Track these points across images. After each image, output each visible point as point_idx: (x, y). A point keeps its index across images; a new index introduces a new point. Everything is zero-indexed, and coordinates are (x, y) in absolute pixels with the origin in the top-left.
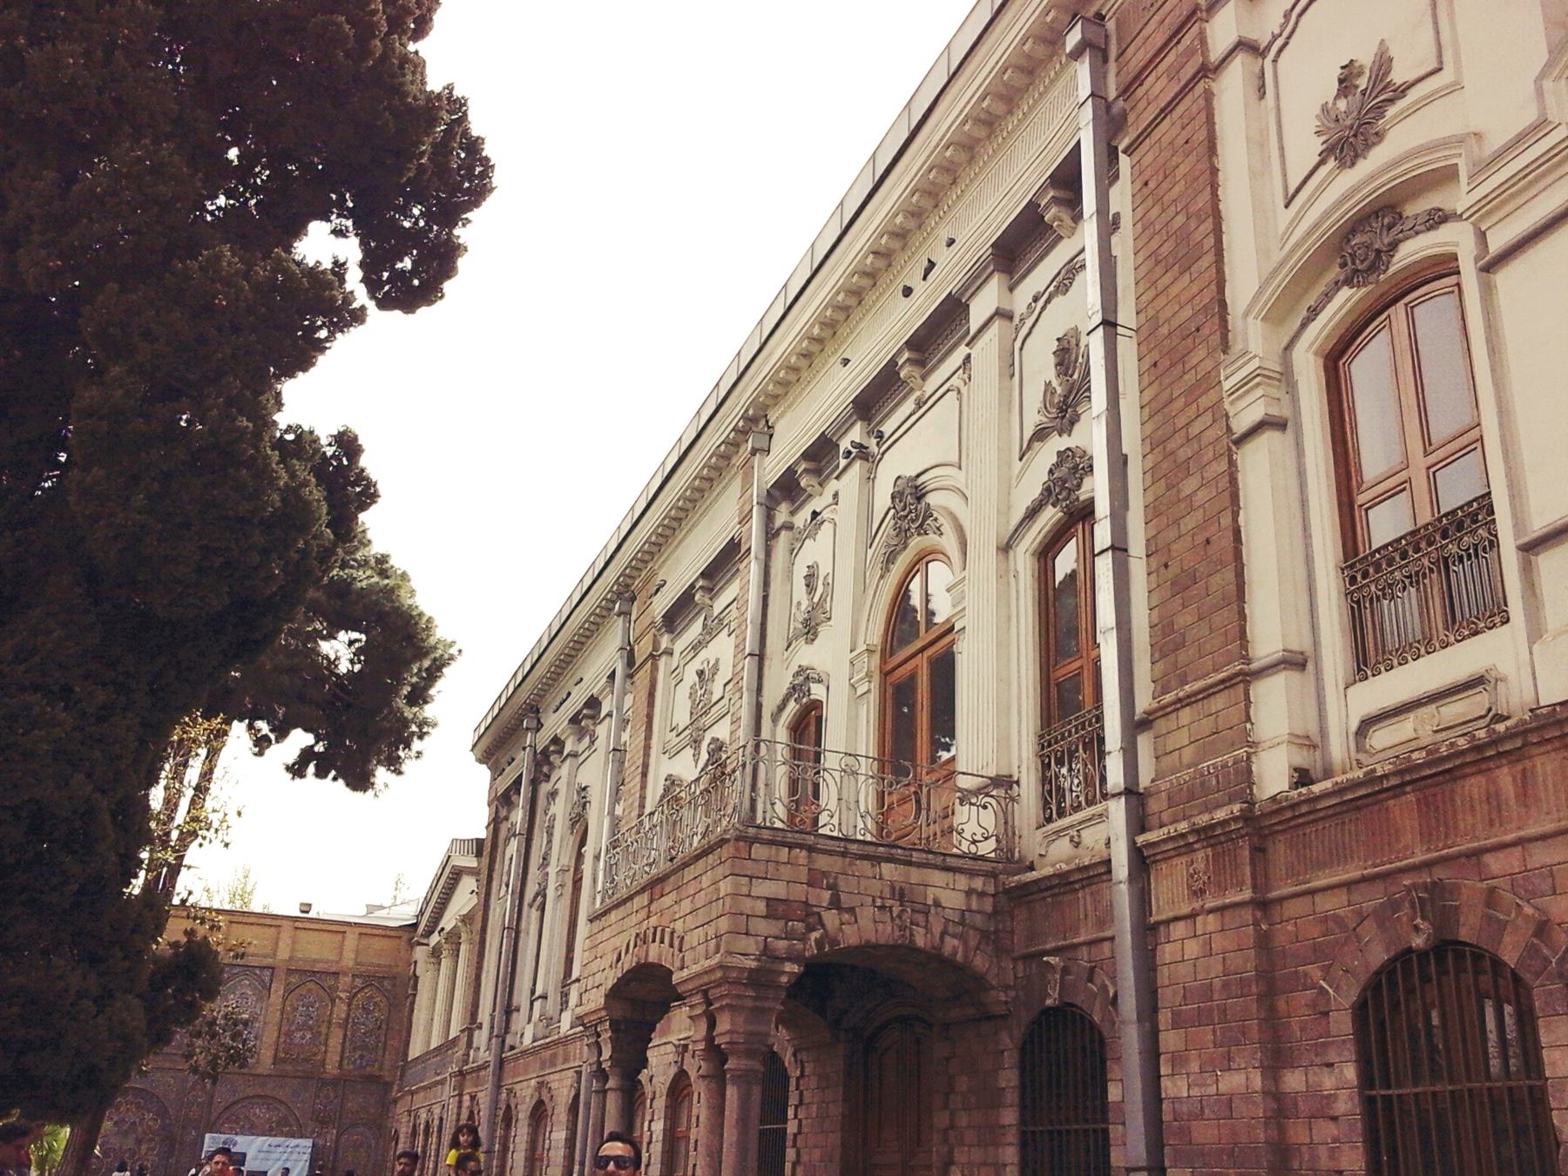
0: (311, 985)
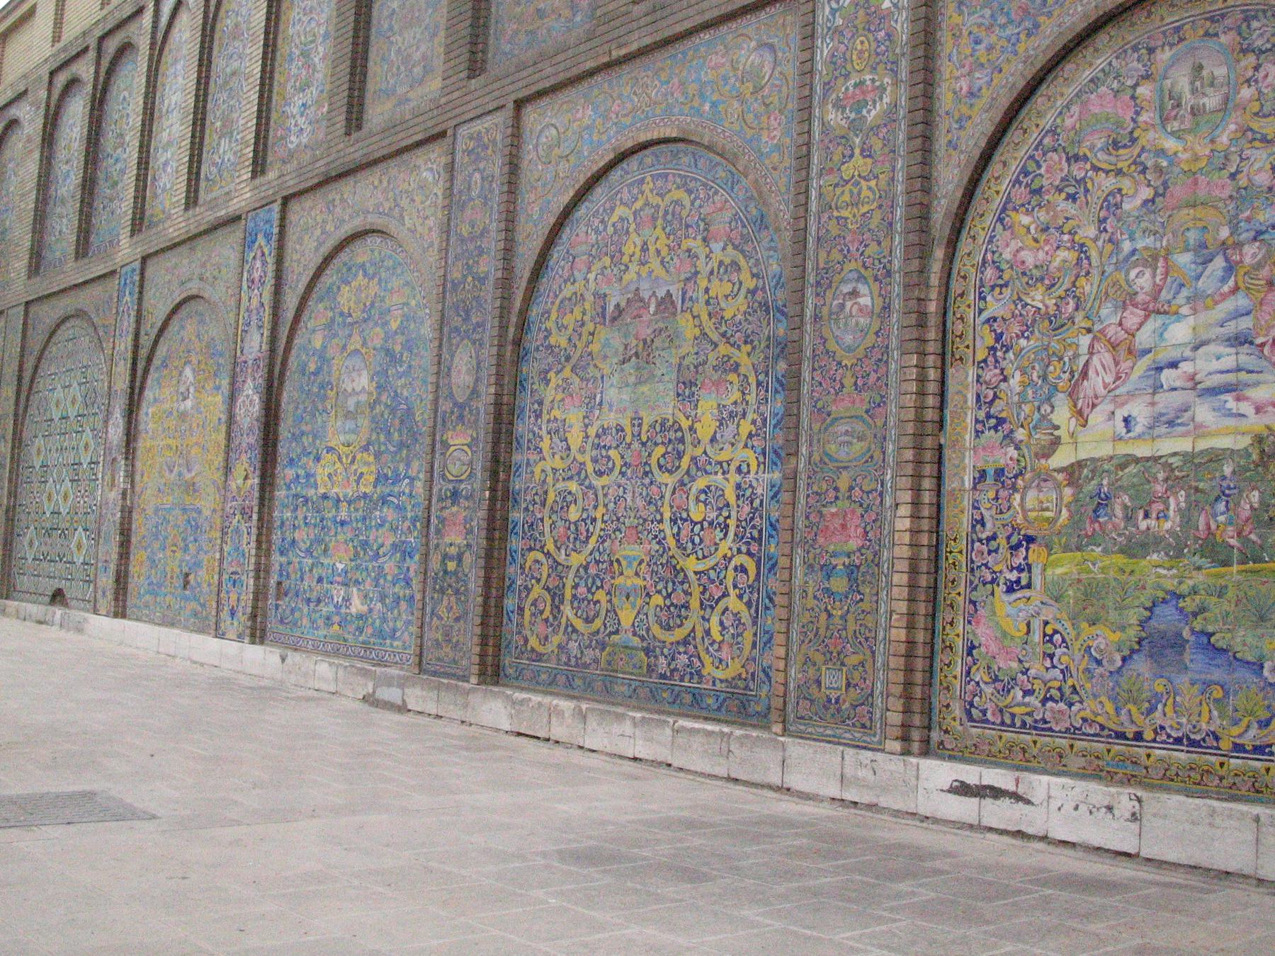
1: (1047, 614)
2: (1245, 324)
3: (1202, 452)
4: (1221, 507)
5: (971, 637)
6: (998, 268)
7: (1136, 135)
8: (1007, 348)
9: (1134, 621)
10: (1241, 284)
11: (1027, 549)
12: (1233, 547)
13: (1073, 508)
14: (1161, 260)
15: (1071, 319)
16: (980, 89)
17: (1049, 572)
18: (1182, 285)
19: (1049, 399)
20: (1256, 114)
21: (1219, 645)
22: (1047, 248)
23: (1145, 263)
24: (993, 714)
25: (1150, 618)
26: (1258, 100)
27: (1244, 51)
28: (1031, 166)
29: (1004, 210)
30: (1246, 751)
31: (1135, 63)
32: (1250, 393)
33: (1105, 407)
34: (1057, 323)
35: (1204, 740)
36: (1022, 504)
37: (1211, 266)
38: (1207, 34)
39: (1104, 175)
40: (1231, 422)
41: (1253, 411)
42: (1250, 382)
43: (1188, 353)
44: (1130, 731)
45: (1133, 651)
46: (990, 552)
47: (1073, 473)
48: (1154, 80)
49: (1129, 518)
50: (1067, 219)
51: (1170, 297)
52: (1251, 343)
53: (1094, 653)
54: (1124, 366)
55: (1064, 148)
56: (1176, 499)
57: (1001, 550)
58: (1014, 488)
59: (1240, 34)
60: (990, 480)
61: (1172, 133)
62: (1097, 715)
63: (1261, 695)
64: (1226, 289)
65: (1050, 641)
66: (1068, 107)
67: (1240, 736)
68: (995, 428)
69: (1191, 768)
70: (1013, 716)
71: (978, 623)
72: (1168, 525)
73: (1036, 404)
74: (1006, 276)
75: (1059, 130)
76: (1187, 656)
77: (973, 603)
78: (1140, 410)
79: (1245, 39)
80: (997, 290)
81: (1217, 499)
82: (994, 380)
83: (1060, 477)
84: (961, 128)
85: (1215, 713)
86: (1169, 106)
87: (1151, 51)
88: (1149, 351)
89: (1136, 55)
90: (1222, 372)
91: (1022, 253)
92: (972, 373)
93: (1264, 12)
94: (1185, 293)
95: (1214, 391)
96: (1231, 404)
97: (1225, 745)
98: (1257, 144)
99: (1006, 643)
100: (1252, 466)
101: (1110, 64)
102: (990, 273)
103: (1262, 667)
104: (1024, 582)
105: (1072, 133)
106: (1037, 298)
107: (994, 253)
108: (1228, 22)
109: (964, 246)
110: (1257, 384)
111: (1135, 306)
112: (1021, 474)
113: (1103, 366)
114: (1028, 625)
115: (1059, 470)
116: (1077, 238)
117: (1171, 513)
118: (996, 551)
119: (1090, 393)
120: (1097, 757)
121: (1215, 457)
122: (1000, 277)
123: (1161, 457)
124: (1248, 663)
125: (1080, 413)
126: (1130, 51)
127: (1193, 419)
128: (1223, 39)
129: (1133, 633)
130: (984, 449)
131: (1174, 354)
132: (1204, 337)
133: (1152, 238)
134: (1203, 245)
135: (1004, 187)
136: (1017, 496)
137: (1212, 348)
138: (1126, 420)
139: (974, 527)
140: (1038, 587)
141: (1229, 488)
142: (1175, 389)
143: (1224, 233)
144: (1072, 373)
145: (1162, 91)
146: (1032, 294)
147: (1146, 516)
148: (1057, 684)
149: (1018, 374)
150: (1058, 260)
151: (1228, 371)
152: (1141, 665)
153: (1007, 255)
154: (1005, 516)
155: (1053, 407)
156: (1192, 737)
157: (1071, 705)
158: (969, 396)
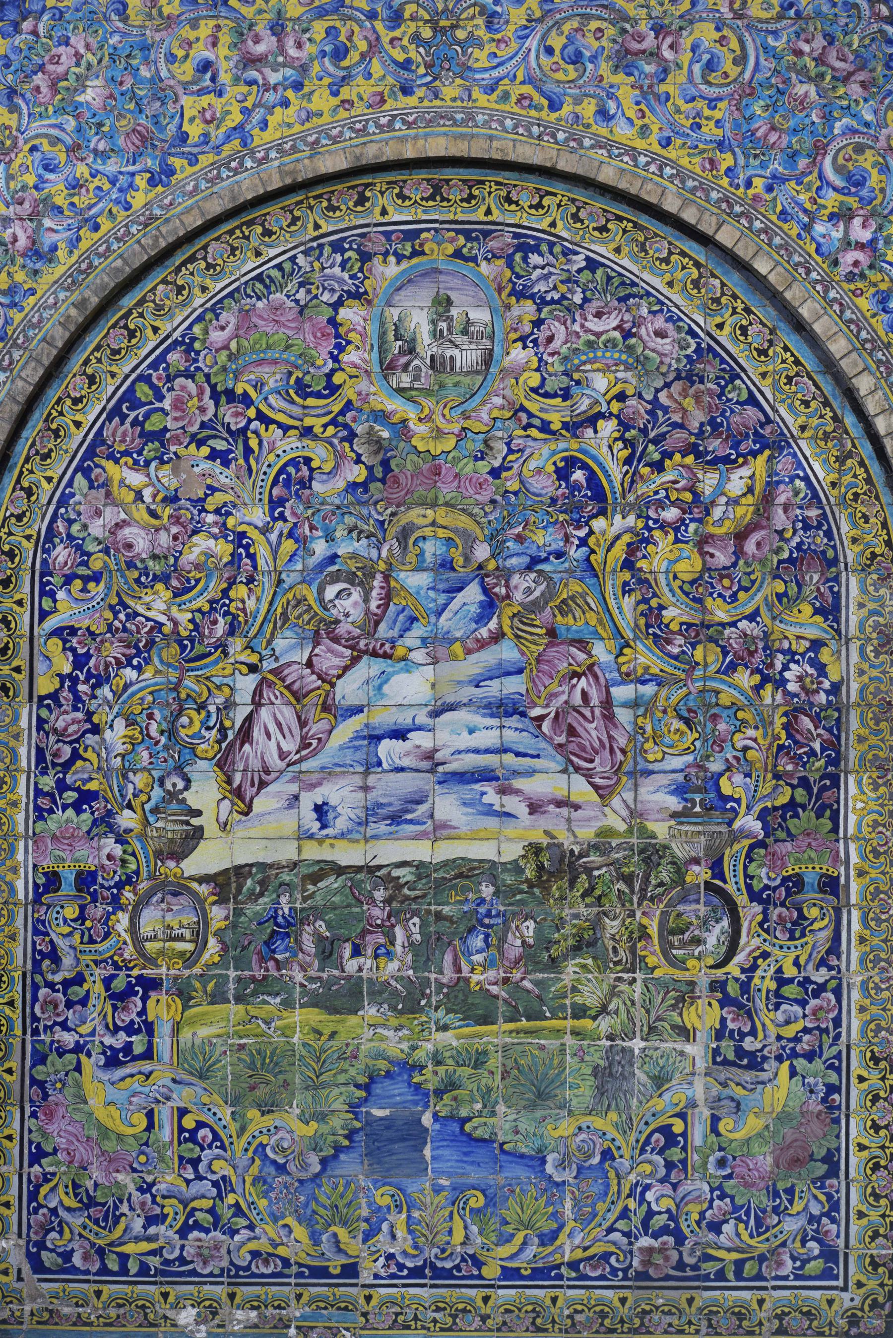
1: (183, 1096)
2: (514, 685)
3: (446, 864)
4: (478, 942)
5: (36, 1137)
6: (79, 548)
7: (337, 379)
9: (339, 1105)
10: (507, 629)
11: (144, 999)
12: (496, 997)
13: (228, 937)
14: (379, 577)
15: (222, 647)
16: (54, 248)
17: (186, 1034)
18: (413, 619)
19: (179, 769)
20: (534, 390)
21: (479, 1133)
22: (174, 530)
23: (351, 579)
24: (86, 1257)
25: (366, 1100)
26: (537, 370)
27: (520, 295)
28: (143, 391)
29: (90, 453)
30: (523, 1278)
31: (337, 270)
32: (518, 783)
33: (281, 788)
35: (458, 1267)
36: (133, 928)
37: (460, 598)
38: (458, 254)
39: (280, 432)
40: (492, 823)
41: (527, 810)
42: (521, 769)
43: (422, 718)
44: (335, 1265)
45: (338, 1149)
46: (69, 1005)
48: (369, 302)
50: (213, 489)
51: (391, 634)
52: (523, 714)
53: (271, 1155)
54: (315, 728)
55: (207, 376)
56: (406, 929)
57: (92, 1001)
58: (116, 902)
59: (510, 265)
60: (67, 888)
61: (400, 391)
62: (275, 1246)
63: (542, 1201)
64: (484, 632)
65: (193, 1139)
67: (512, 1257)
68: (77, 806)
69: (439, 1309)
70: (124, 1258)
71: (50, 1115)
72: (393, 966)
73: (156, 774)
74: (96, 564)
75: (197, 345)
76: (427, 1152)
77: (41, 1084)
79: (519, 277)
80: (78, 584)
81: (471, 930)
82: (71, 729)
83: (203, 890)
84: (14, 305)
85: (475, 1229)
87: (365, 257)
88: (359, 710)
89: (339, 258)
90: (477, 751)
91: (127, 531)
93: (551, 245)
94: (418, 630)
95: (462, 778)
96: (491, 797)
97: (491, 1271)
98: (534, 432)
99: (110, 1146)
100: (524, 887)
101: (293, 259)
102: (61, 554)
103: (543, 1161)
104: (138, 1049)
105: (223, 357)
107: (70, 522)
108: (493, 244)
110: (531, 773)
111: (336, 640)
112: (129, 881)
113: (279, 725)
114: (150, 1115)
115: (203, 879)
116: (231, 522)
117: (399, 949)
118: (84, 1002)
119: (255, 764)
120: (279, 1307)
122: (85, 564)
123: (379, 867)
124: (522, 1156)
125: (238, 793)
126: (327, 250)
127: (432, 816)
128: (484, 268)
130: (54, 837)
131: (404, 719)
132: (450, 699)
133: (364, 542)
134: (447, 565)
135: (91, 418)
136: (123, 920)
137: (462, 716)
138: (320, 810)
139: (37, 964)
140: (166, 1058)
141: (488, 915)
142: (402, 770)
143: (482, 552)
144: (223, 731)
145: (382, 324)
146: (147, 599)
147: (357, 952)
148: (207, 1204)
149: (119, 724)
150: (197, 550)
151: (487, 751)
153: (97, 529)
154: (101, 947)
155: (188, 781)
156: (439, 1264)
157: (233, 1232)
158: (23, 751)
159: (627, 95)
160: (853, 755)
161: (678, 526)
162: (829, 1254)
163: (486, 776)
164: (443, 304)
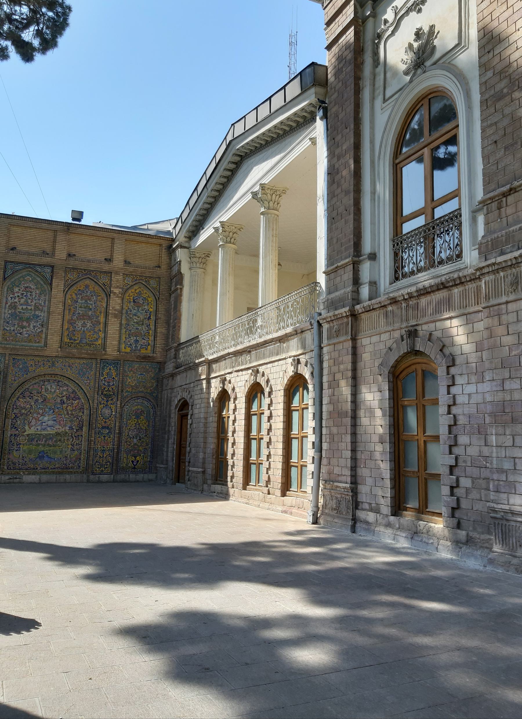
0: (88, 282)
2: (55, 418)
8: (18, 417)
28: (23, 393)
34: (27, 415)
47: (28, 435)
49: (37, 441)
60: (13, 436)
66: (31, 386)
78: (39, 428)
86: (47, 390)
92: (10, 421)
97: (50, 468)
106: (23, 411)
109: (10, 401)
121: (50, 434)
129: (37, 456)
131: (45, 421)
143: (53, 407)
152: (38, 459)
153: (18, 404)
159: (69, 369)
160: (84, 425)
161: (71, 405)
162: (79, 467)
163: (52, 426)
164: (51, 386)
